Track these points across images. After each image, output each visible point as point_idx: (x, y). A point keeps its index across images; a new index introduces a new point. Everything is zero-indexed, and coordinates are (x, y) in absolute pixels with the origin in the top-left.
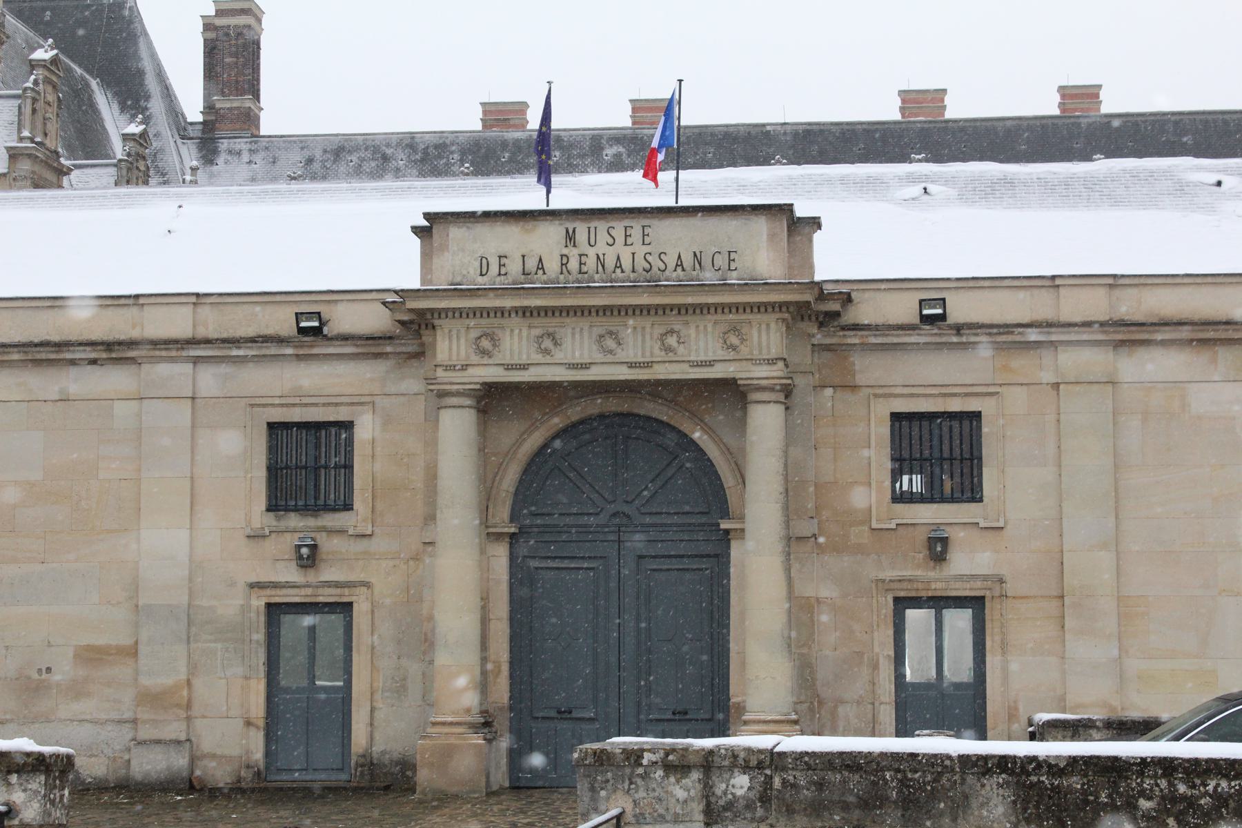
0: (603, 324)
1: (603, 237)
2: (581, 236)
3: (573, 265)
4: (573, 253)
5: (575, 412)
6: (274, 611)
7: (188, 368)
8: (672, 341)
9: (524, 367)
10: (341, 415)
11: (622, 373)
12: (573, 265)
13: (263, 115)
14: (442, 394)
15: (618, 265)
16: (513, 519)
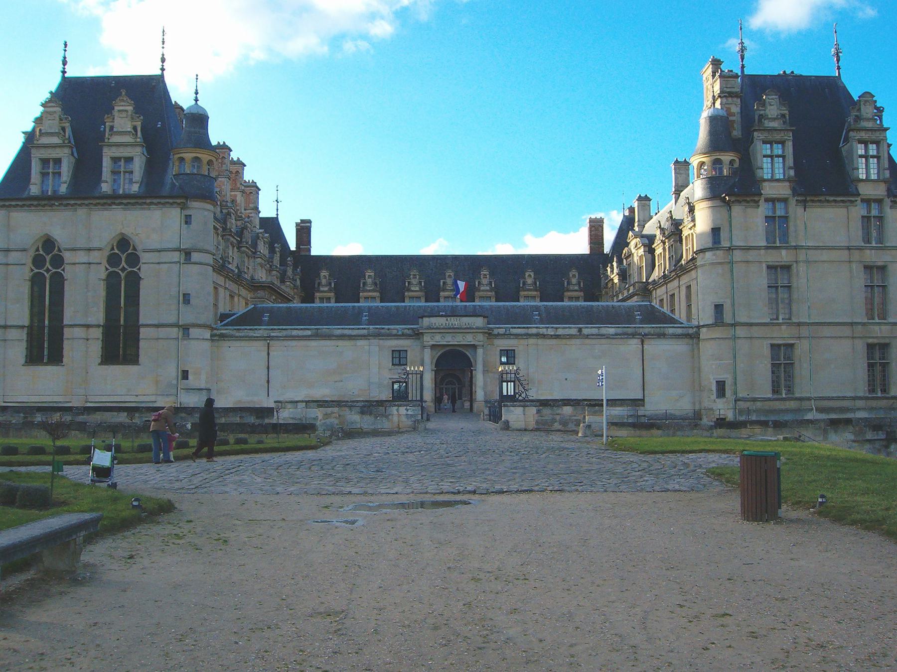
0: (453, 334)
1: (452, 320)
2: (449, 320)
3: (447, 325)
4: (447, 322)
5: (448, 349)
6: (393, 383)
7: (378, 340)
8: (464, 338)
9: (439, 342)
10: (405, 349)
11: (456, 343)
12: (447, 325)
13: (312, 249)
14: (424, 346)
15: (455, 325)
16: (435, 367)
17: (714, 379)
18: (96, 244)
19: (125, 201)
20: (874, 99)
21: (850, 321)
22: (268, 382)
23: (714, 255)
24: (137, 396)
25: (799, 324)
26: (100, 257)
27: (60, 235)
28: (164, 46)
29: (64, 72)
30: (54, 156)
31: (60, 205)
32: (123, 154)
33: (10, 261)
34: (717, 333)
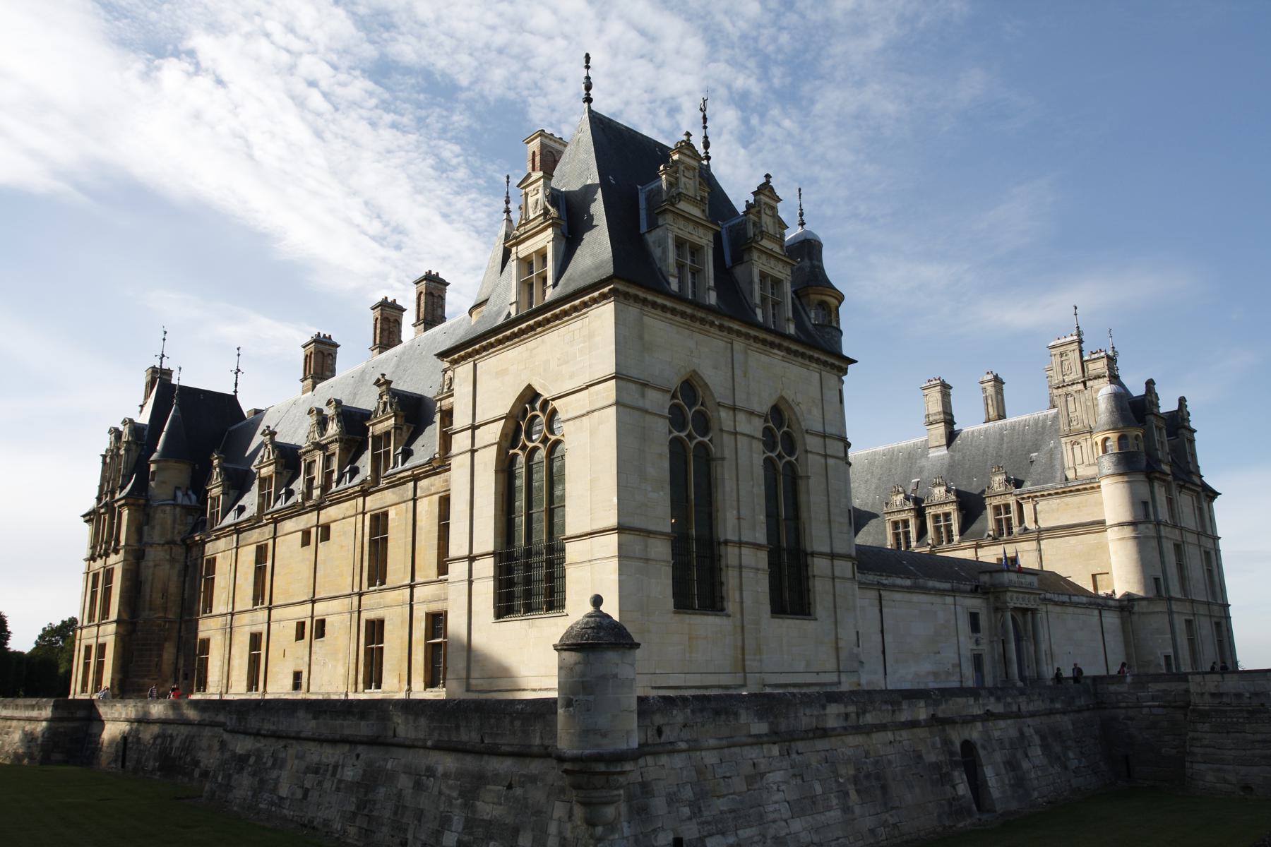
17: (1161, 654)
18: (756, 407)
19: (794, 347)
20: (1186, 403)
21: (1206, 600)
22: (884, 652)
23: (1147, 528)
24: (818, 673)
25: (1193, 601)
26: (757, 427)
27: (715, 379)
28: (707, 125)
29: (588, 100)
30: (695, 239)
31: (721, 327)
32: (774, 271)
33: (648, 405)
34: (1161, 607)
